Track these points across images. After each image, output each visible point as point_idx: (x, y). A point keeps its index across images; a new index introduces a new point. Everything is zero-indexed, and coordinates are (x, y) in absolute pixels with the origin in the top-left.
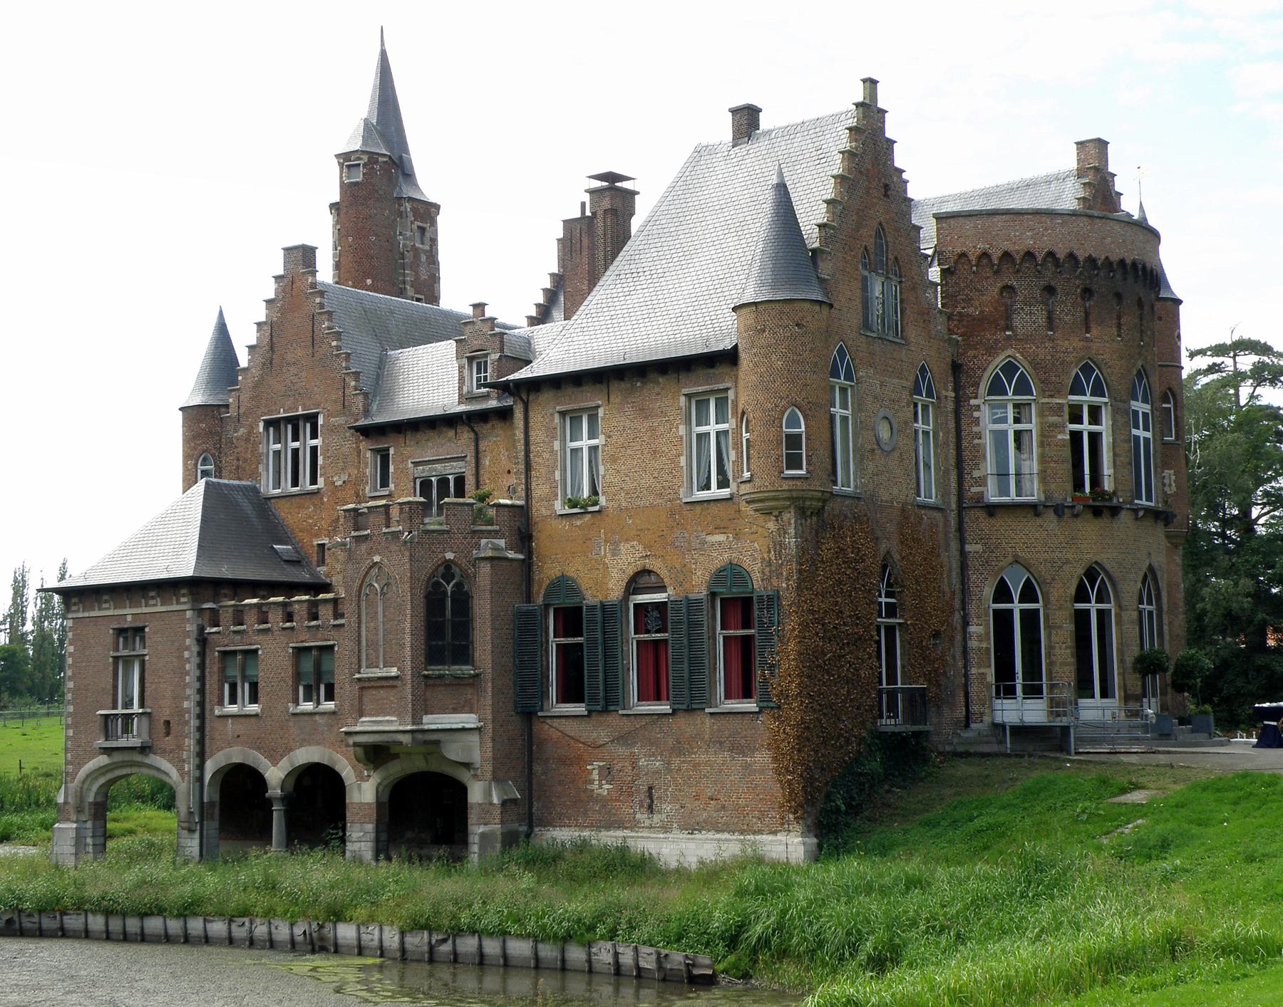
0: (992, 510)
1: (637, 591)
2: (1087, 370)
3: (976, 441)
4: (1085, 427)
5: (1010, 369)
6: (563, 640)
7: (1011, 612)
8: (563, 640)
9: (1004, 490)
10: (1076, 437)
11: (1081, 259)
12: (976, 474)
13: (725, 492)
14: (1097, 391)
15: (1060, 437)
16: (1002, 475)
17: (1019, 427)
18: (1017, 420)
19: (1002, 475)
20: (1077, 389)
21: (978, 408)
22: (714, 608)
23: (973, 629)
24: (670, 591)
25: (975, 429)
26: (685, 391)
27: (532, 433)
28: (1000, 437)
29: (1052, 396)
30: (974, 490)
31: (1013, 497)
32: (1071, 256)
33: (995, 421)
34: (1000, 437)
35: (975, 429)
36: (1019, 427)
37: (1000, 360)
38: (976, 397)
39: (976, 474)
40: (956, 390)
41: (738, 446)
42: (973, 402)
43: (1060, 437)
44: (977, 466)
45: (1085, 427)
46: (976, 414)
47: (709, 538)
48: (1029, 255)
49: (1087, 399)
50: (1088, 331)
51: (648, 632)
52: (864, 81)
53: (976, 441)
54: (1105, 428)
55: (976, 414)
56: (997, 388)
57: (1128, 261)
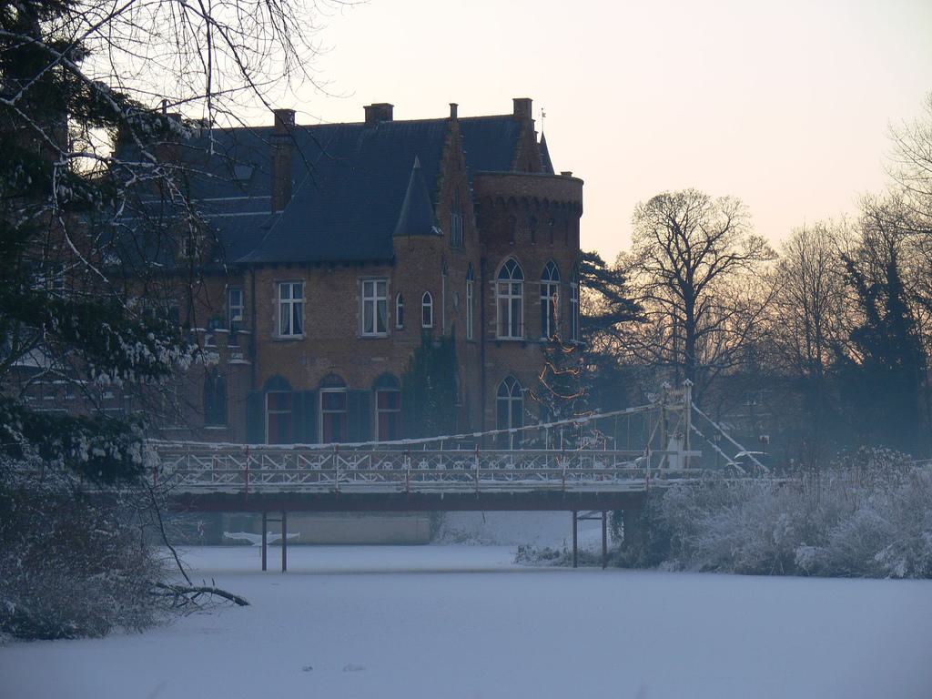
0: (499, 344)
1: (324, 386)
2: (550, 265)
3: (491, 304)
4: (548, 298)
5: (511, 264)
6: (274, 412)
7: (507, 401)
8: (274, 412)
9: (505, 333)
10: (544, 302)
11: (550, 202)
12: (491, 323)
13: (382, 335)
14: (555, 278)
15: (536, 303)
16: (505, 325)
17: (515, 297)
18: (513, 293)
19: (505, 325)
20: (545, 276)
21: (493, 285)
22: (374, 395)
23: (487, 411)
24: (349, 386)
25: (491, 297)
26: (360, 277)
27: (257, 293)
28: (504, 303)
29: (532, 280)
30: (490, 332)
31: (510, 337)
32: (546, 199)
33: (502, 293)
34: (504, 303)
35: (491, 297)
36: (515, 297)
37: (507, 258)
38: (493, 279)
39: (491, 323)
40: (482, 274)
41: (392, 310)
42: (491, 282)
43: (536, 303)
44: (491, 319)
45: (548, 298)
46: (492, 289)
47: (374, 359)
48: (524, 199)
49: (548, 283)
50: (552, 243)
51: (332, 409)
52: (451, 105)
53: (491, 304)
54: (556, 299)
55: (492, 289)
56: (504, 275)
57: (572, 202)
